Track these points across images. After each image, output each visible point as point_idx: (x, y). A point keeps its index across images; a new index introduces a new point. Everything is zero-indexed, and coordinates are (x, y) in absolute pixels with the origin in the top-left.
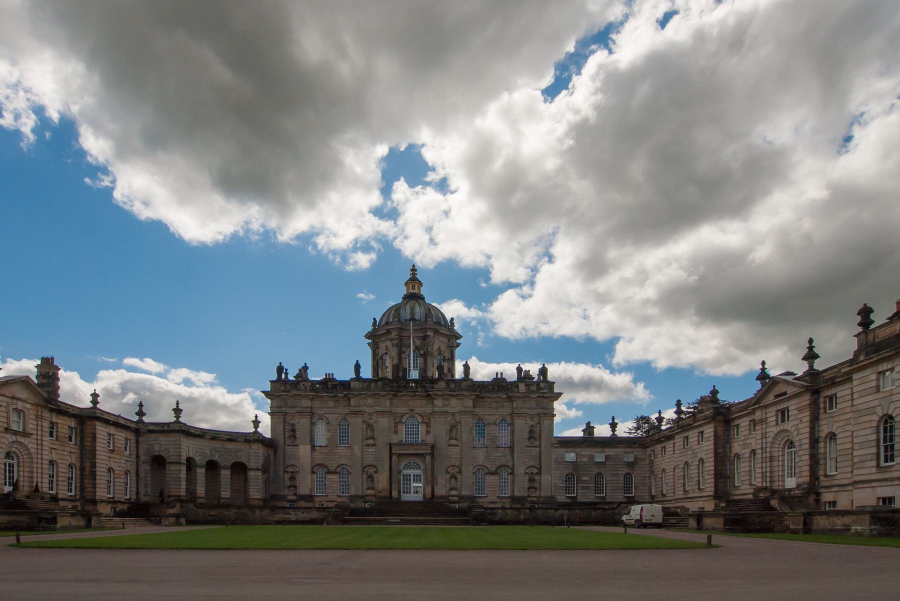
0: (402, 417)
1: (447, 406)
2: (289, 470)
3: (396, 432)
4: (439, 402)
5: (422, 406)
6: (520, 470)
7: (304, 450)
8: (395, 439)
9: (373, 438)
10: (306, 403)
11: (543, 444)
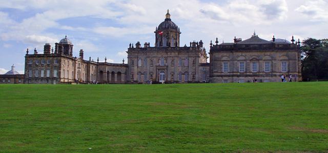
4: (169, 54)
6: (190, 73)
7: (136, 68)
8: (158, 64)
10: (136, 54)
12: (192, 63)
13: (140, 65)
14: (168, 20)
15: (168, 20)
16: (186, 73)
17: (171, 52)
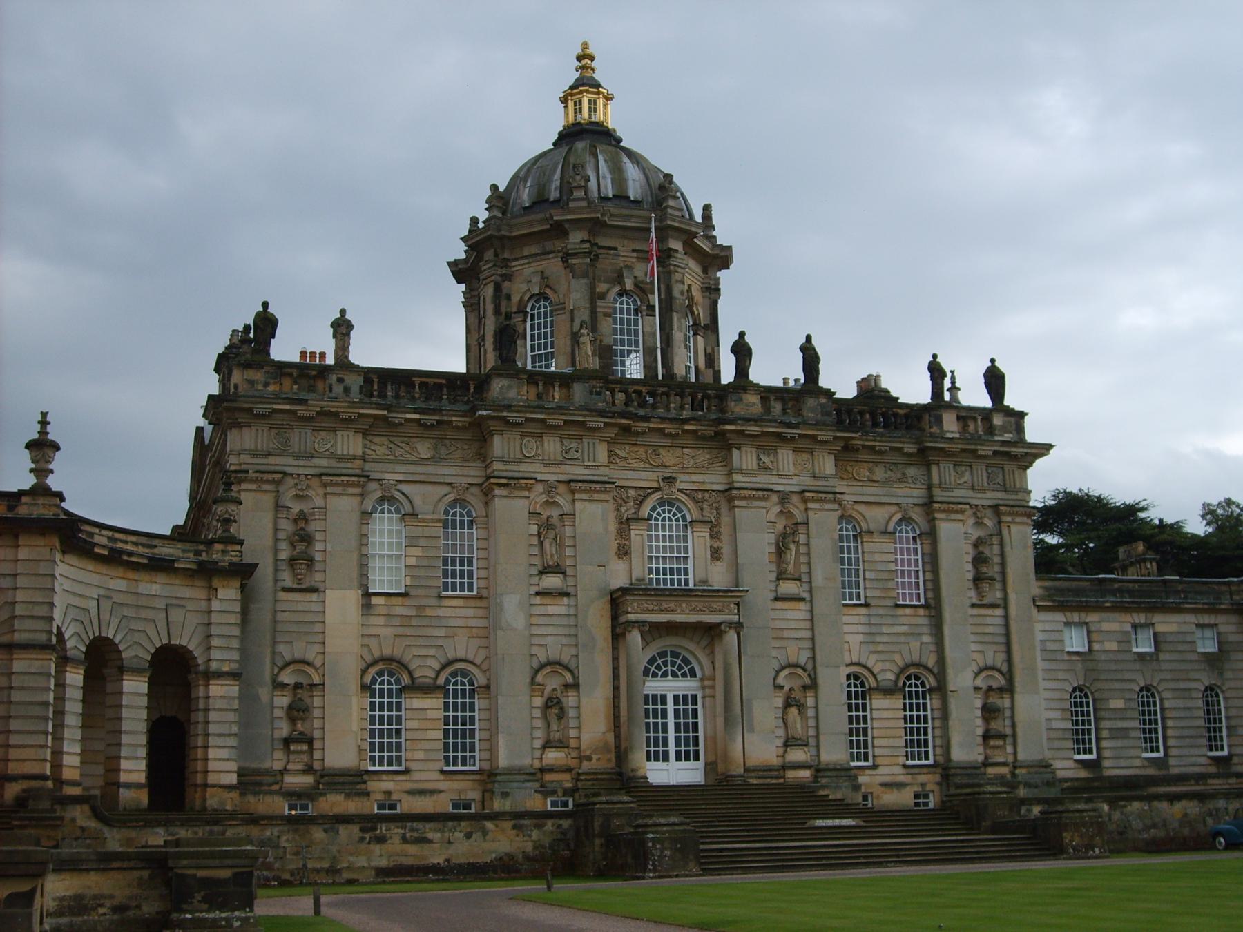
0: (640, 503)
1: (765, 469)
2: (287, 678)
3: (624, 552)
4: (745, 458)
5: (698, 473)
6: (961, 680)
7: (340, 605)
9: (558, 569)
10: (349, 443)
11: (1012, 597)
12: (968, 571)
13: (385, 578)
14: (585, 136)
15: (585, 136)
16: (922, 684)
17: (768, 443)
